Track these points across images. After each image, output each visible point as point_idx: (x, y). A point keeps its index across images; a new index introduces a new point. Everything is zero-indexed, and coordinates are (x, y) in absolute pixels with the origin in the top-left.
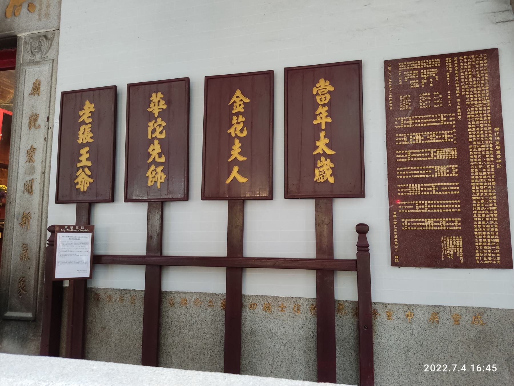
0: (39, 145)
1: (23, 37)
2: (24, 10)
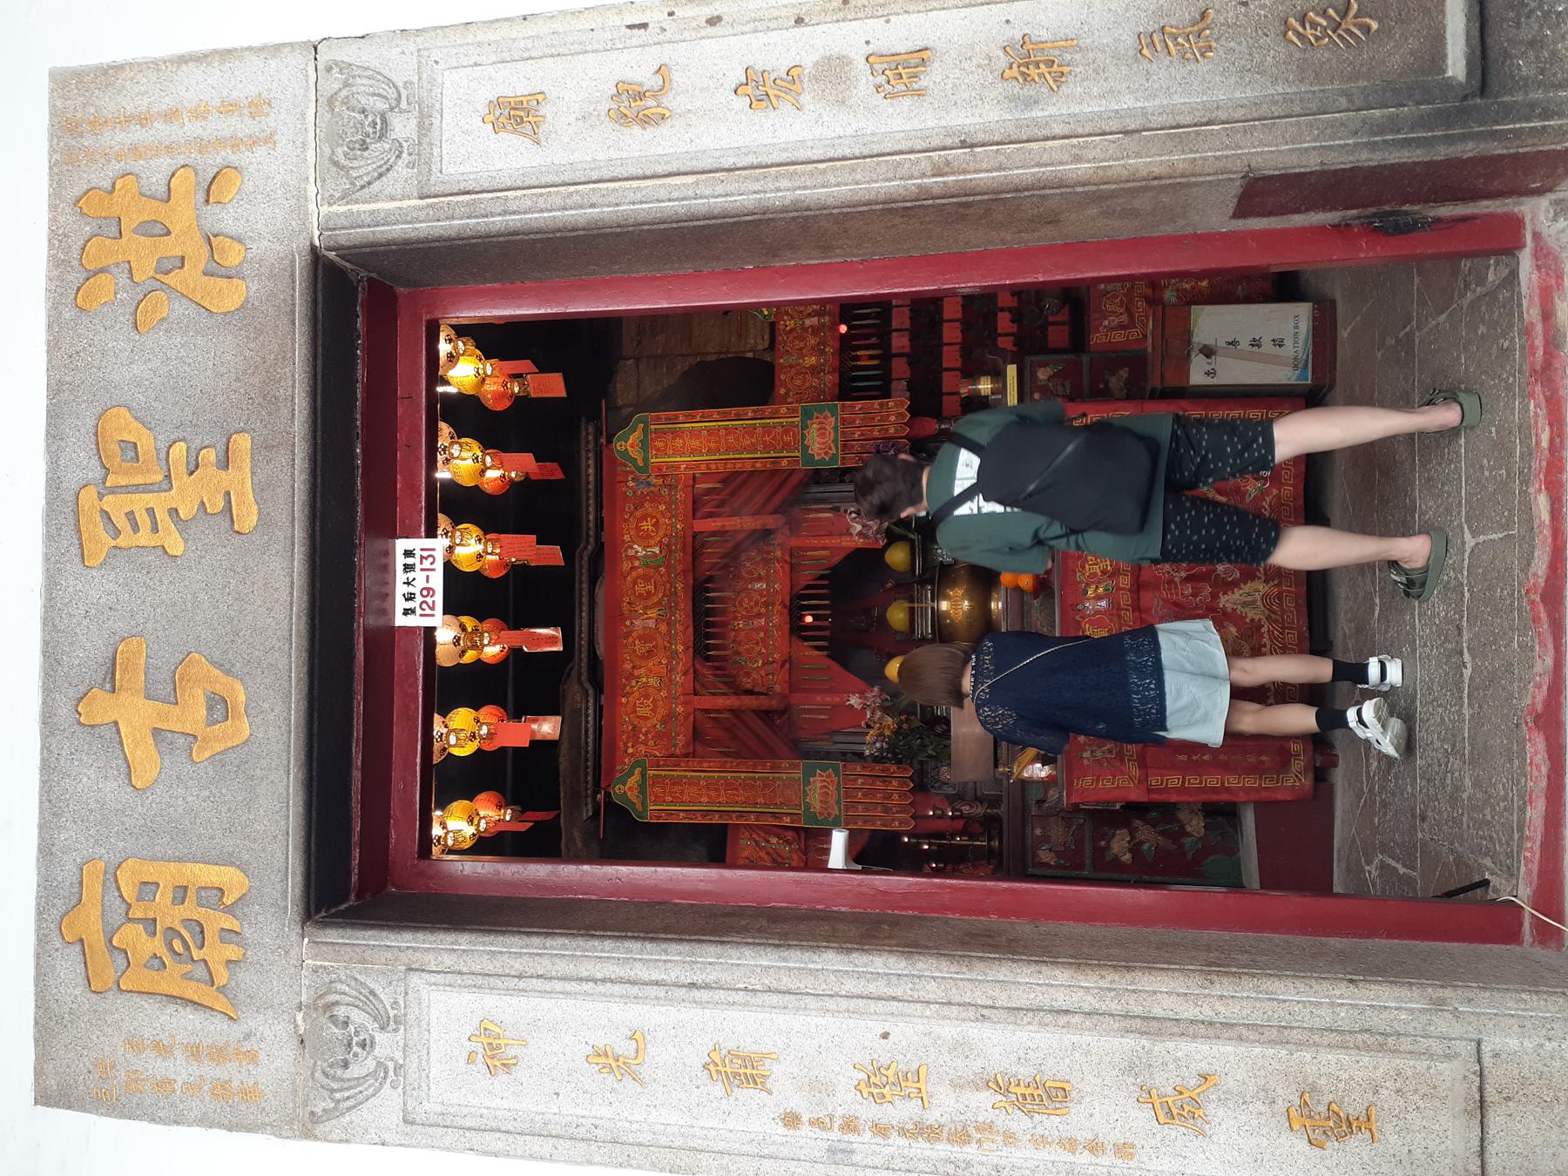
0: (729, 55)
1: (324, 209)
2: (226, 218)
